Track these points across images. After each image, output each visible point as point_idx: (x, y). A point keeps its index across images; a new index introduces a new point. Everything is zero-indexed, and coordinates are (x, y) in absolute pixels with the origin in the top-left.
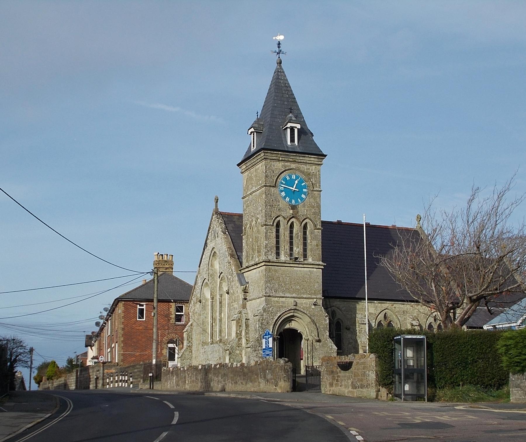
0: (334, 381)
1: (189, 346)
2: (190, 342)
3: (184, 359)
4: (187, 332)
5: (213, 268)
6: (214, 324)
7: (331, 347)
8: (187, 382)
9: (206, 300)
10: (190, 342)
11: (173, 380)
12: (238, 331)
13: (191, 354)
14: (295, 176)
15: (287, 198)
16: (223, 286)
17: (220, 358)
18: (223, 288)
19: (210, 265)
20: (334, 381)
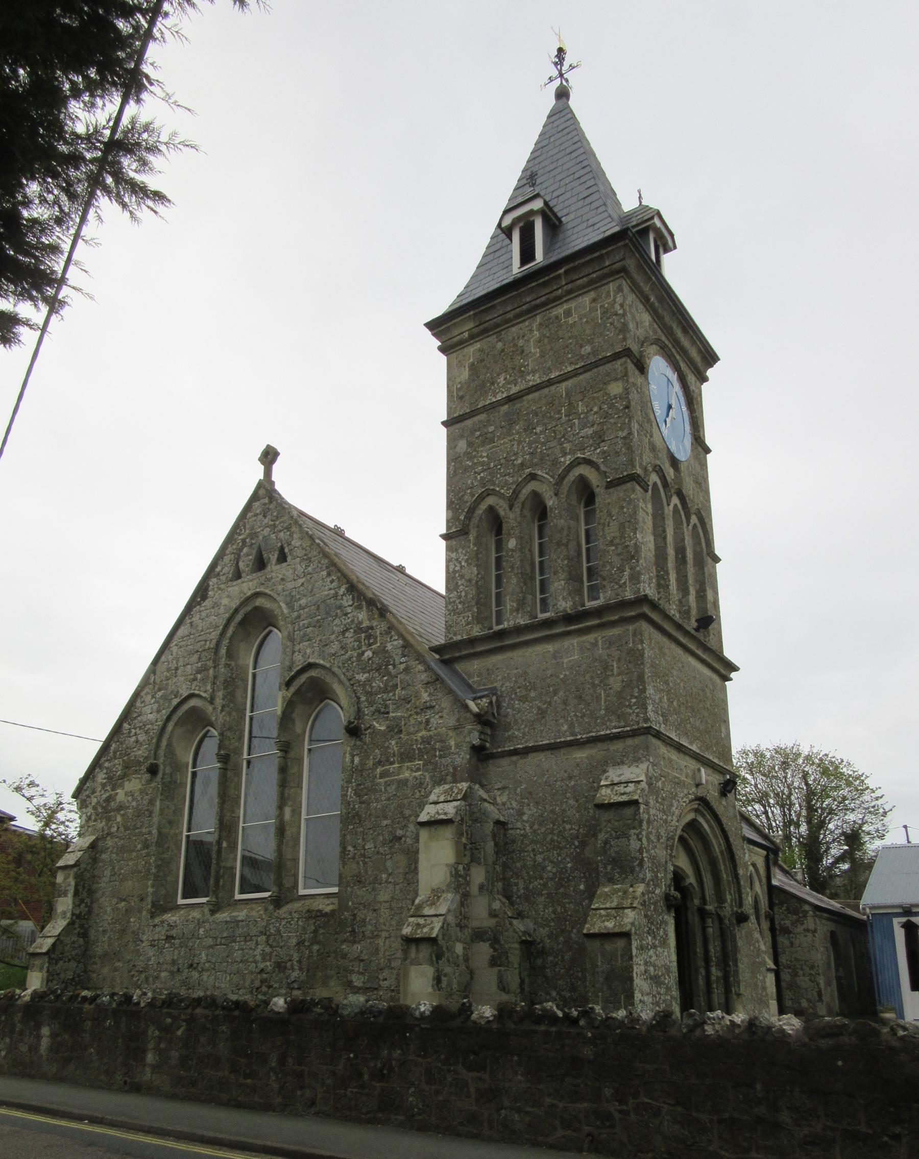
1: (79, 916)
2: (82, 901)
3: (60, 959)
4: (75, 869)
5: (233, 663)
6: (224, 844)
8: (150, 1057)
9: (178, 767)
10: (82, 901)
11: (39, 1037)
12: (461, 867)
13: (81, 941)
16: (294, 715)
17: (280, 966)
18: (293, 720)
19: (223, 651)
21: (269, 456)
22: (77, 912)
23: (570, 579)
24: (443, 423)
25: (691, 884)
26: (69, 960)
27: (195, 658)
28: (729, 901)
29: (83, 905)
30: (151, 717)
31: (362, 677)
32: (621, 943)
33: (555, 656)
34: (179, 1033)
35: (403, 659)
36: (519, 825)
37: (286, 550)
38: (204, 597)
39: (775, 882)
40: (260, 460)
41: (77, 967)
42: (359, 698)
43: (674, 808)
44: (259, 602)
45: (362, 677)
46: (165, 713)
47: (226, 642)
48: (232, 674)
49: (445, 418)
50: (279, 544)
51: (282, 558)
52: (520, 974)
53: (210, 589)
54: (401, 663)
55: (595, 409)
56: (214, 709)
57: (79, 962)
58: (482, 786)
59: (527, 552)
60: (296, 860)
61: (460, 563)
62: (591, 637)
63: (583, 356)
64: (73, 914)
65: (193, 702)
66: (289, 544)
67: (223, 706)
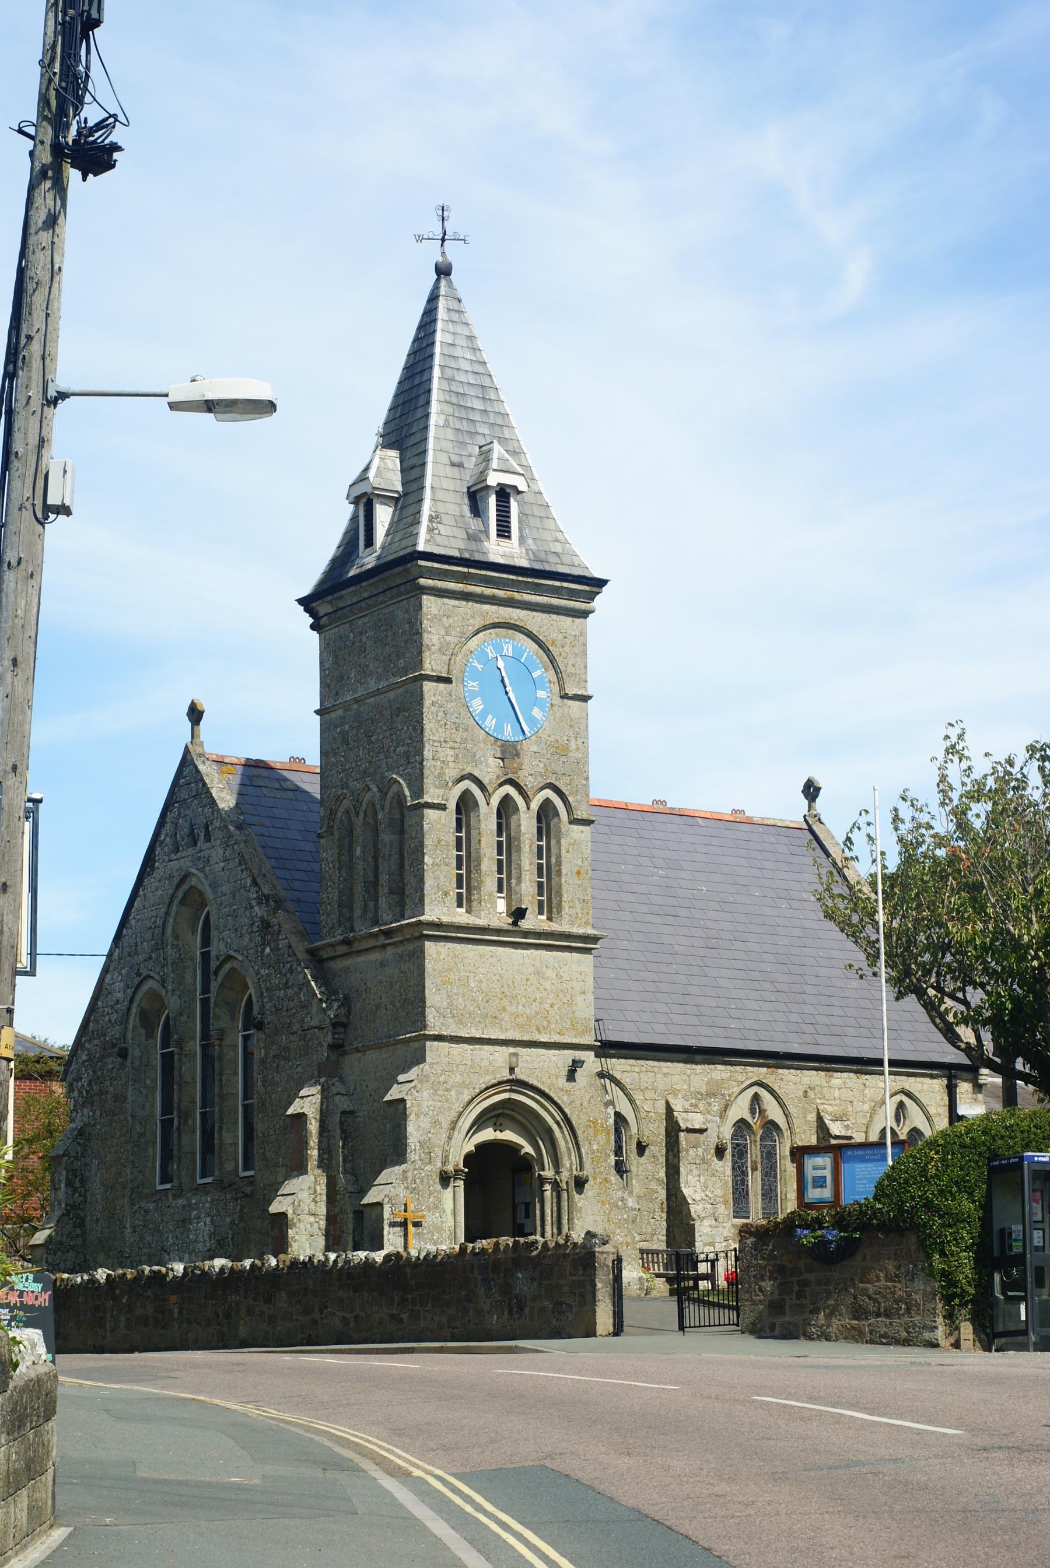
0: (788, 1298)
1: (74, 1207)
7: (620, 1203)
13: (78, 1231)
14: (510, 647)
15: (490, 717)
20: (788, 1298)
21: (195, 714)
22: (71, 1202)
23: (390, 893)
24: (317, 712)
25: (526, 1153)
26: (68, 1251)
27: (148, 935)
28: (568, 1166)
29: (77, 1194)
30: (119, 995)
31: (264, 972)
32: (379, 1208)
33: (383, 964)
34: (124, 1301)
35: (289, 959)
36: (361, 1114)
37: (210, 829)
38: (153, 869)
39: (961, 1111)
40: (188, 714)
41: (76, 1257)
42: (262, 993)
43: (465, 1096)
44: (194, 881)
45: (264, 972)
46: (130, 991)
47: (171, 920)
48: (180, 955)
49: (318, 707)
50: (205, 821)
51: (208, 838)
52: (354, 1237)
53: (157, 858)
54: (288, 962)
55: (405, 728)
56: (167, 991)
57: (78, 1253)
58: (342, 1080)
59: (370, 859)
60: (236, 1144)
61: (328, 863)
62: (400, 950)
63: (399, 669)
64: (67, 1205)
65: (150, 984)
66: (212, 823)
67: (173, 991)
